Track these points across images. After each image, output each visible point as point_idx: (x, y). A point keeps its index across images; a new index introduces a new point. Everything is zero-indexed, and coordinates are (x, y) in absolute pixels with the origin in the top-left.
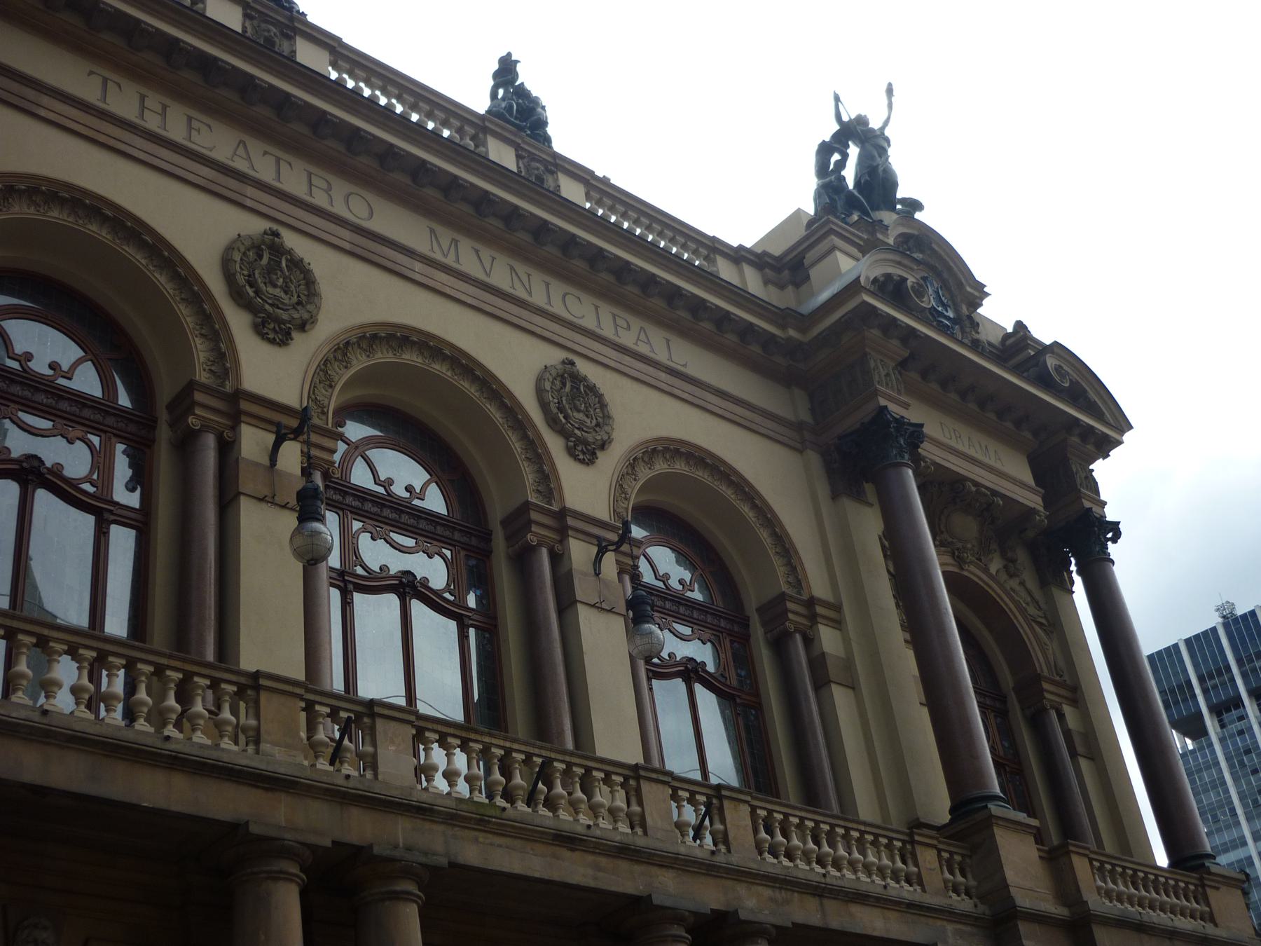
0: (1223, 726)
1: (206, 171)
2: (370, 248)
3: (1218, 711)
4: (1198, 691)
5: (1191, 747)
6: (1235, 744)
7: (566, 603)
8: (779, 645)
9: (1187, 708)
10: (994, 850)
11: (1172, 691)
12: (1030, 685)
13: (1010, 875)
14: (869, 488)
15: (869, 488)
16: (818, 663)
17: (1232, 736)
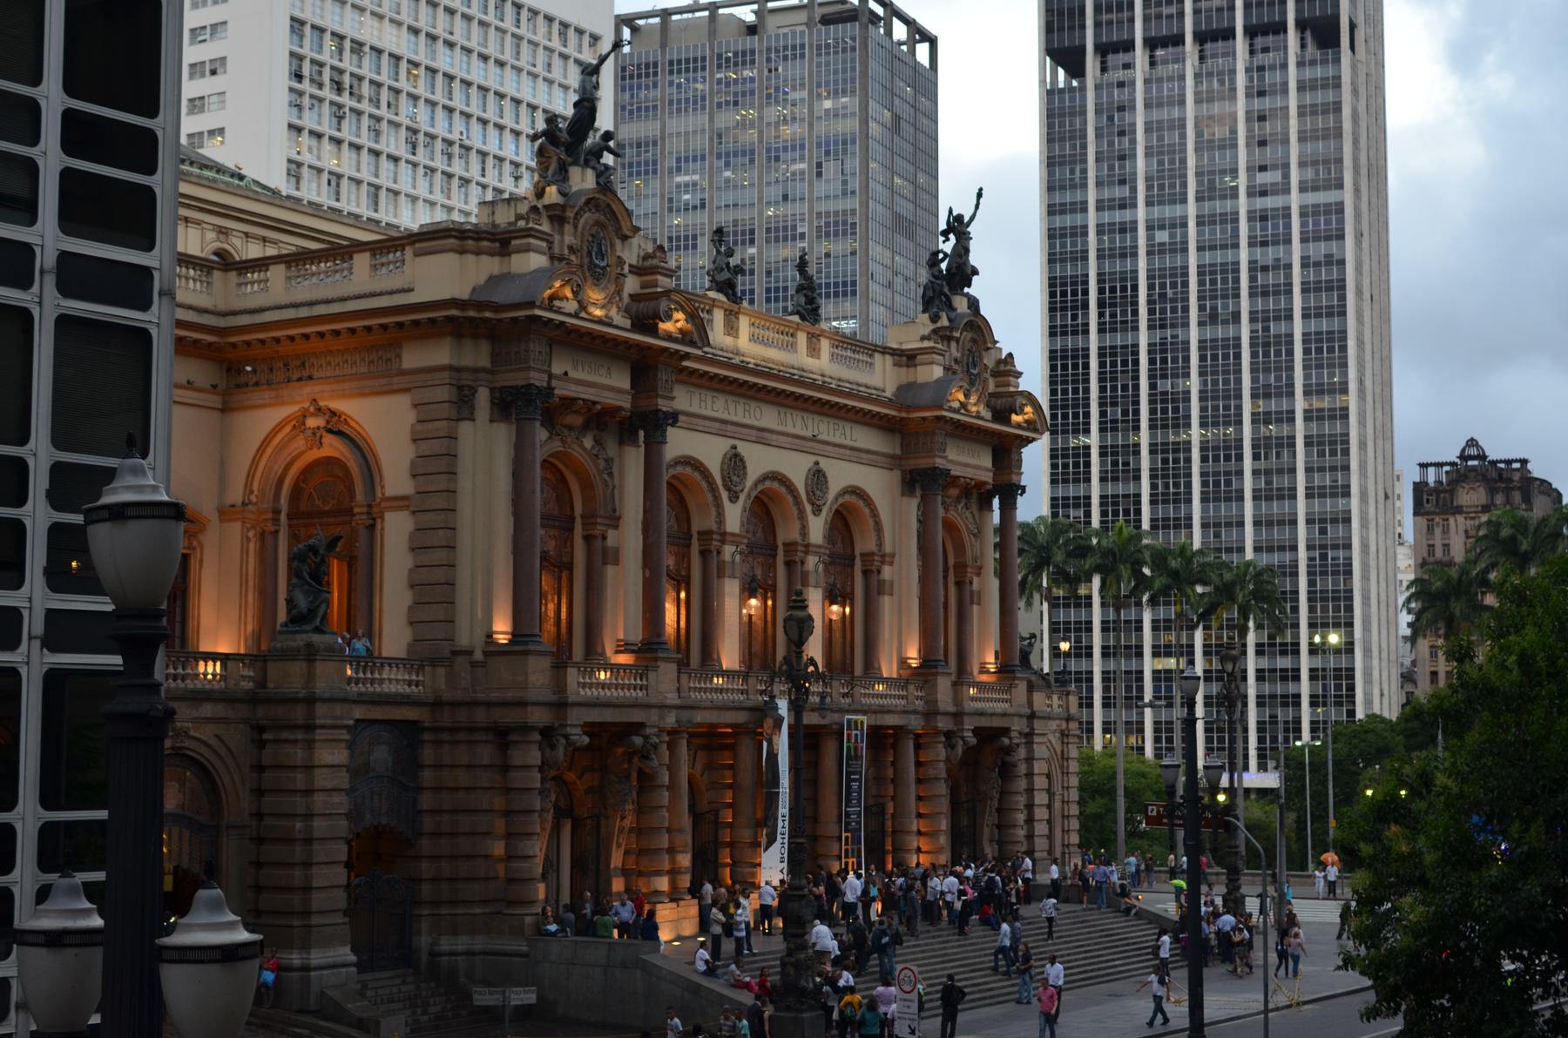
0: (1104, 69)
1: (717, 425)
2: (762, 436)
3: (1103, 50)
4: (1089, 22)
5: (1061, 85)
6: (1110, 95)
7: (805, 583)
8: (866, 573)
9: (1071, 38)
10: (935, 685)
11: (1061, 13)
12: (961, 567)
13: (940, 697)
14: (918, 487)
15: (918, 493)
16: (881, 583)
17: (1110, 85)
